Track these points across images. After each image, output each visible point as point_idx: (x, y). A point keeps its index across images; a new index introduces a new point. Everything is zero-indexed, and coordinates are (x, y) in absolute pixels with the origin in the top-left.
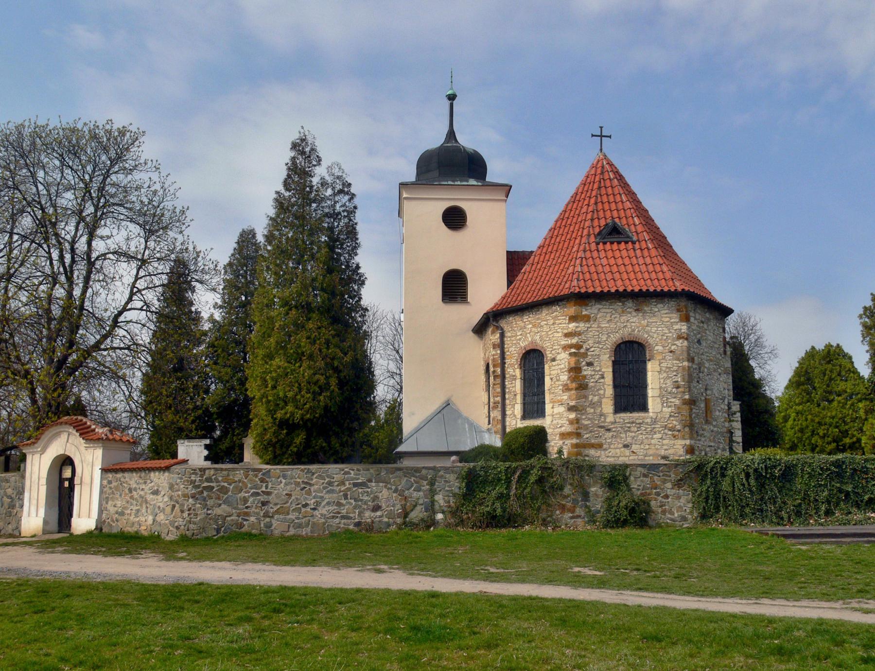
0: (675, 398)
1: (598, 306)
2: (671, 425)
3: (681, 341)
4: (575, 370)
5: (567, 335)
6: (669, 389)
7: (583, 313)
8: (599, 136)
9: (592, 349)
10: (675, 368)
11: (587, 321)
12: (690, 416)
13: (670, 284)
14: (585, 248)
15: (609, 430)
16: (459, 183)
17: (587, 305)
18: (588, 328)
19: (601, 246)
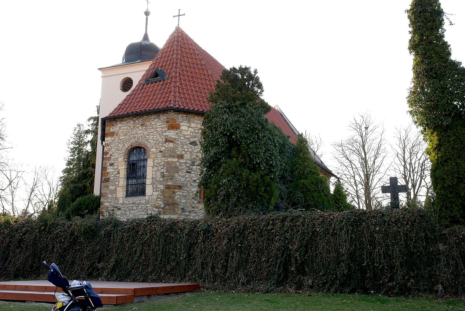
0: (161, 184)
1: (119, 125)
2: (157, 205)
3: (167, 143)
6: (158, 179)
7: (111, 131)
8: (177, 16)
10: (162, 163)
15: (119, 209)
17: (113, 125)
18: (113, 140)
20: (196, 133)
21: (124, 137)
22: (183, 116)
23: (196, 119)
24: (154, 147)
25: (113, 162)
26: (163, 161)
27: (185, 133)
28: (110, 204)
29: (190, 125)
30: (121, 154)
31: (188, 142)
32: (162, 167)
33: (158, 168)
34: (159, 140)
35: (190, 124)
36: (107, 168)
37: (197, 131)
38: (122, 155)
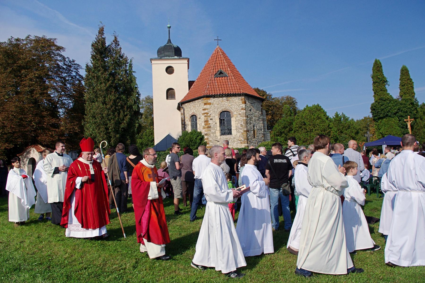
2: (240, 139)
3: (243, 110)
4: (206, 121)
5: (204, 110)
6: (239, 127)
7: (209, 102)
9: (212, 114)
10: (241, 120)
12: (247, 136)
13: (239, 91)
14: (210, 79)
15: (219, 141)
16: (171, 58)
19: (216, 79)
21: (217, 106)
25: (212, 118)
28: (213, 139)
32: (241, 121)
36: (209, 121)
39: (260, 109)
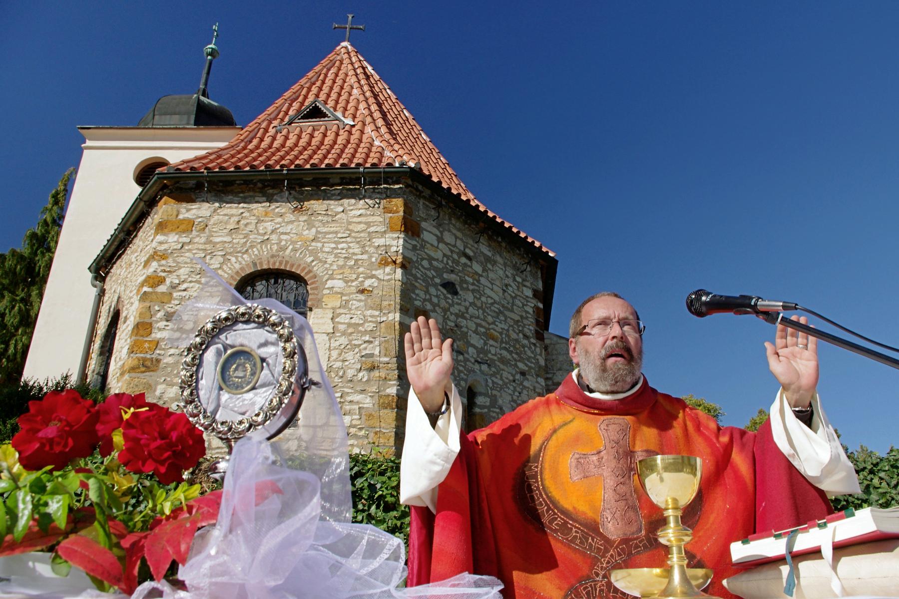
0: (363, 391)
3: (388, 269)
6: (350, 373)
7: (181, 217)
10: (369, 326)
11: (184, 232)
17: (193, 201)
20: (454, 261)
21: (228, 239)
22: (427, 206)
23: (454, 225)
24: (341, 277)
26: (370, 319)
27: (432, 254)
29: (442, 234)
30: (212, 286)
31: (438, 281)
32: (367, 338)
33: (351, 341)
34: (359, 257)
35: (441, 233)
37: (455, 256)
38: (215, 289)
39: (531, 311)
